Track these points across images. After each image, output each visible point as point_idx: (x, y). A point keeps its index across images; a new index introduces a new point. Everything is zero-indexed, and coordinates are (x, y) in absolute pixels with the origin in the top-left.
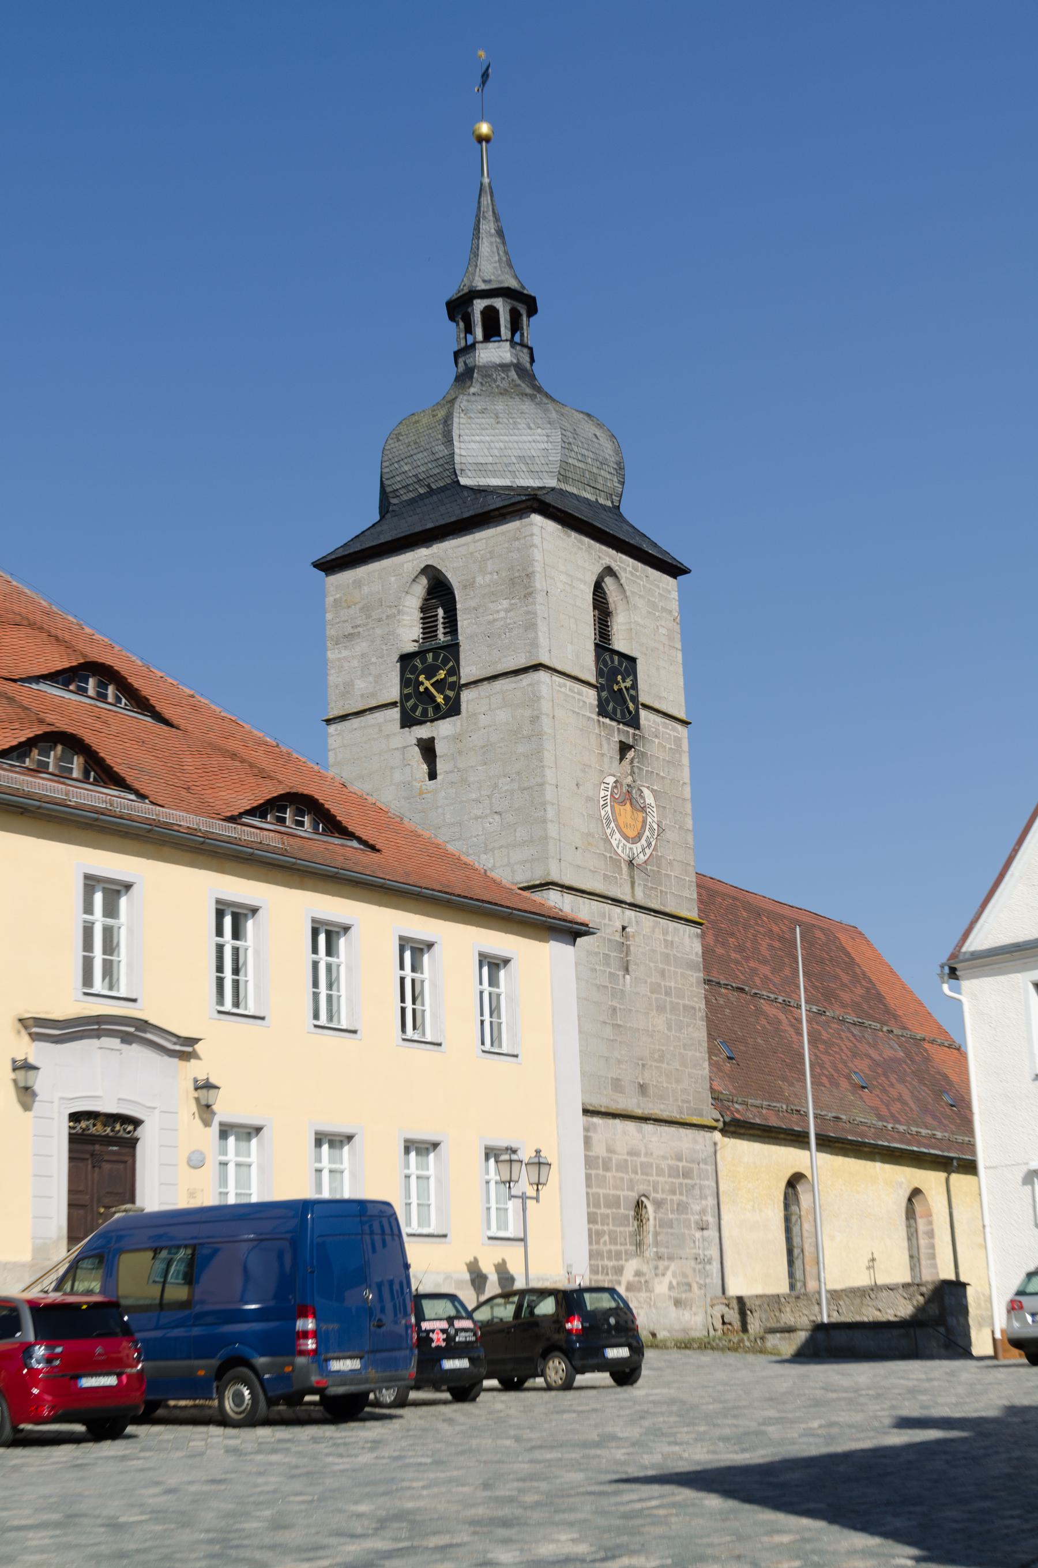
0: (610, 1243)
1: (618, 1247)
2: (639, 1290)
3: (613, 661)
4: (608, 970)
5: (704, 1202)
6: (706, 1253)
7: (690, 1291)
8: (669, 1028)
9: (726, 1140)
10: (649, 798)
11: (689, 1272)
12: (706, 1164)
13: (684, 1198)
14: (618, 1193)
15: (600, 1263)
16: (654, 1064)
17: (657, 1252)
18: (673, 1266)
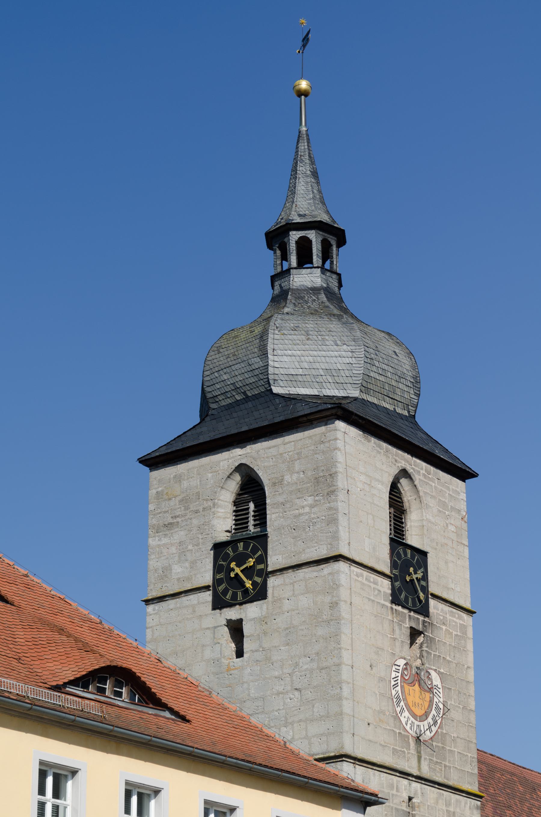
3: (405, 554)
10: (436, 680)
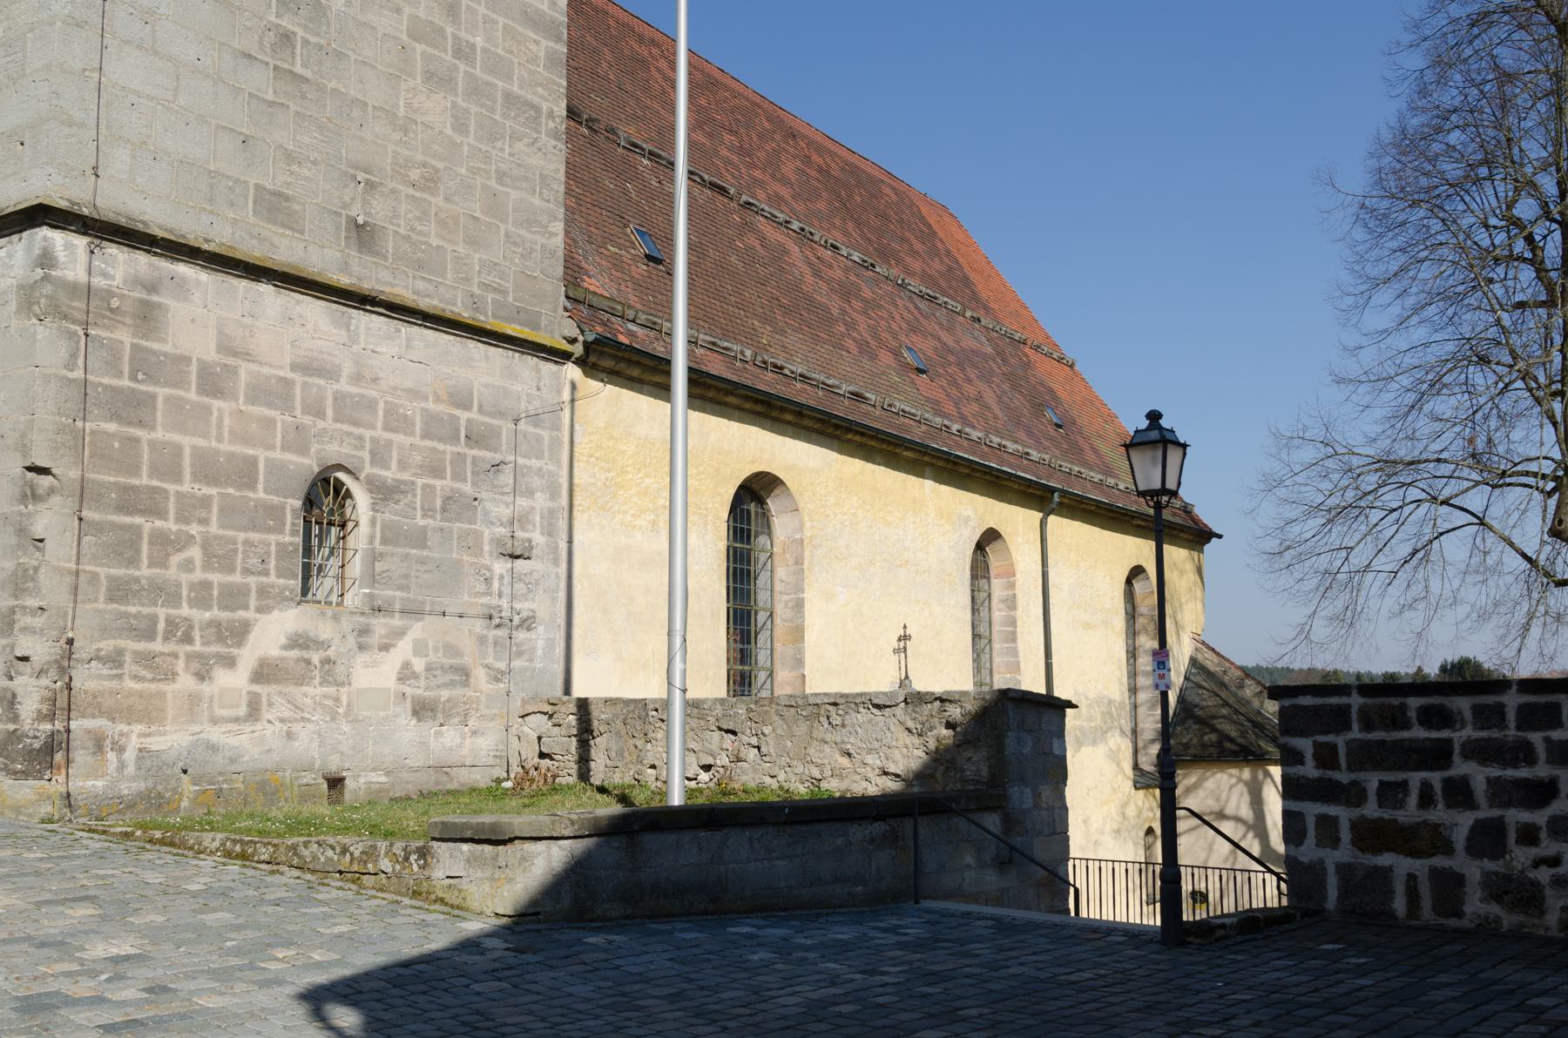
0: (207, 566)
1: (237, 578)
2: (301, 680)
5: (522, 502)
6: (518, 606)
7: (466, 683)
8: (461, 127)
9: (594, 384)
11: (468, 645)
12: (536, 425)
13: (467, 488)
14: (251, 452)
15: (162, 613)
17: (371, 597)
18: (417, 630)
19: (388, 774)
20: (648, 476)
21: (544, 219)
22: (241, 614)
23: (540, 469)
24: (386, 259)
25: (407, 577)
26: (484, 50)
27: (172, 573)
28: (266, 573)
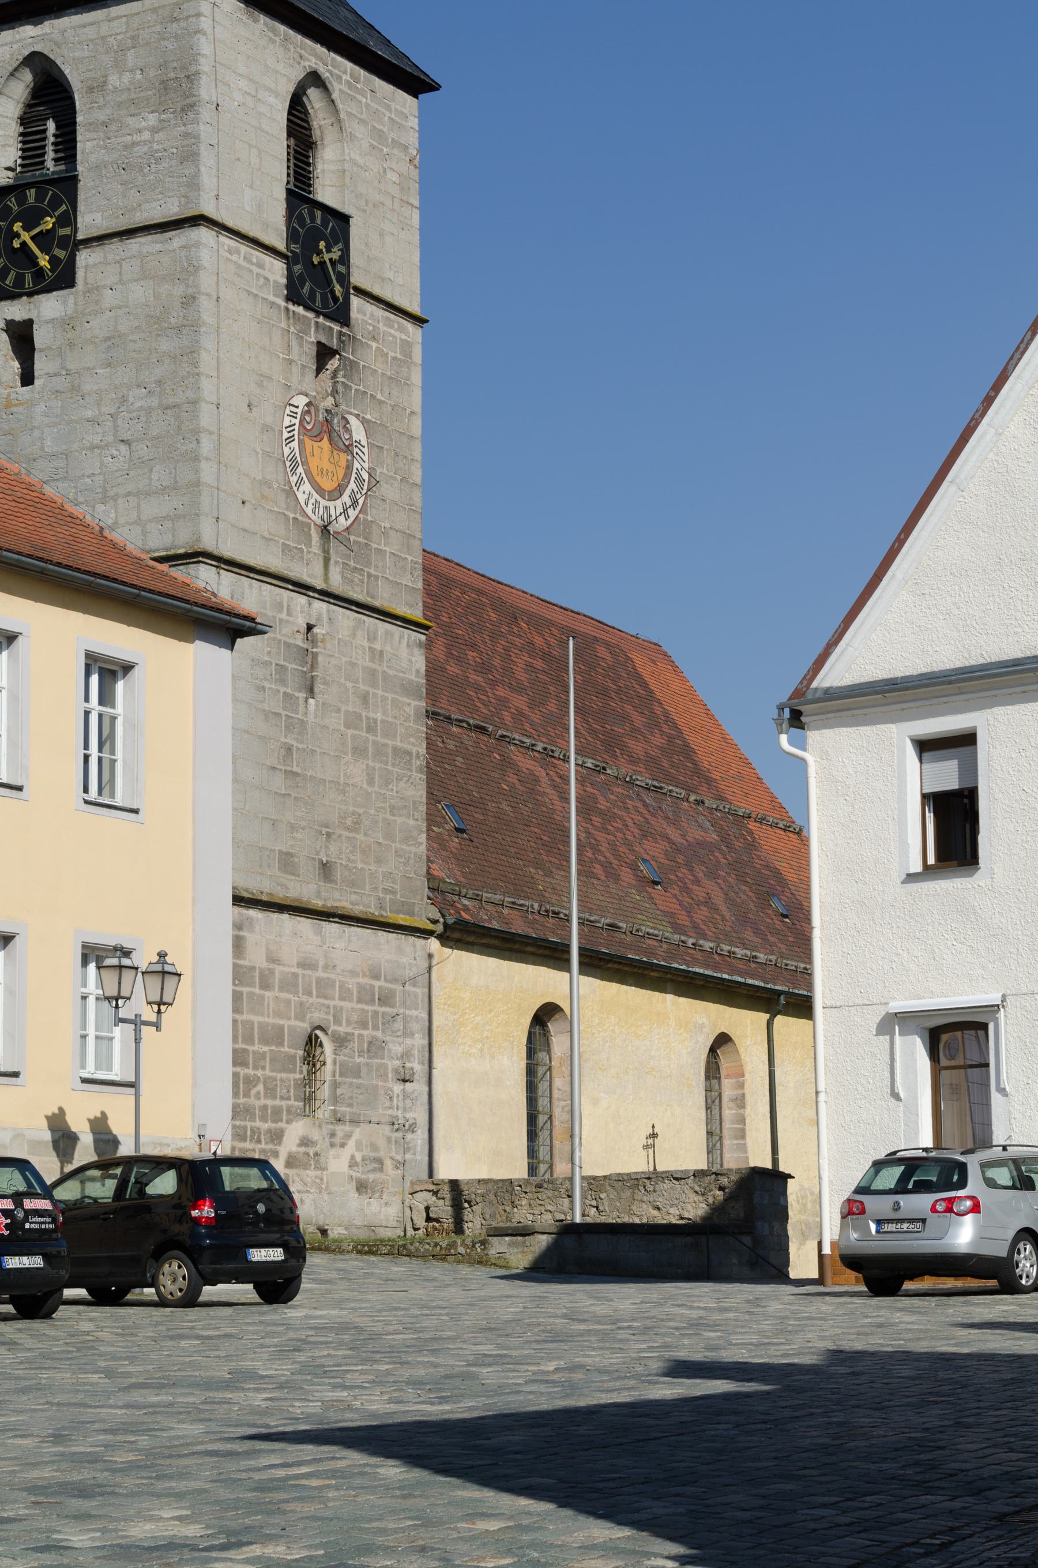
1: (278, 1102)
2: (306, 1166)
3: (313, 218)
4: (283, 689)
5: (408, 1041)
6: (407, 1116)
7: (381, 1170)
8: (371, 782)
9: (447, 951)
11: (382, 1143)
12: (414, 986)
13: (379, 1034)
14: (281, 1022)
15: (249, 1124)
16: (346, 834)
17: (334, 1111)
18: (358, 1133)
19: (346, 1229)
20: (477, 1015)
21: (415, 833)
22: (280, 1125)
23: (417, 1017)
24: (336, 884)
25: (351, 1098)
26: (383, 721)
27: (252, 1101)
28: (289, 1099)
